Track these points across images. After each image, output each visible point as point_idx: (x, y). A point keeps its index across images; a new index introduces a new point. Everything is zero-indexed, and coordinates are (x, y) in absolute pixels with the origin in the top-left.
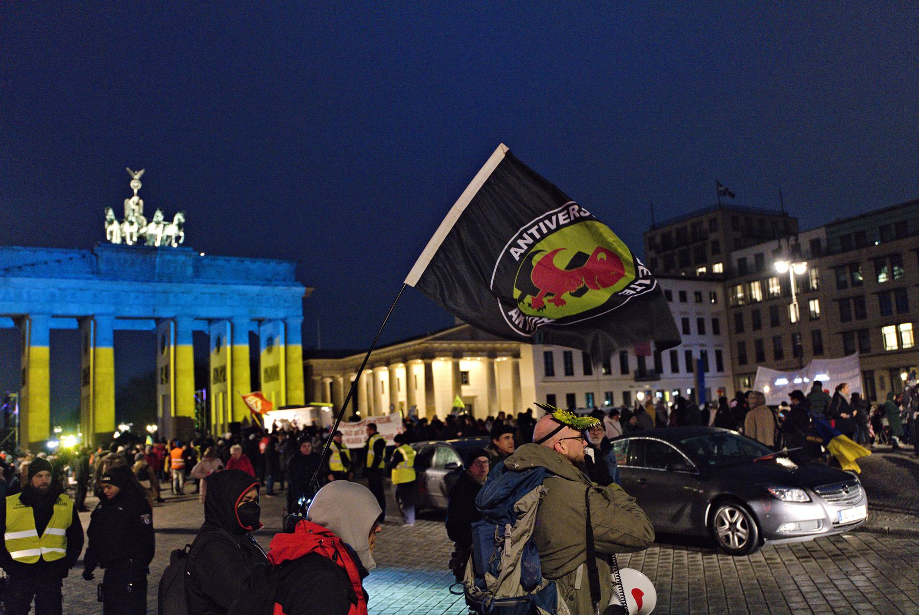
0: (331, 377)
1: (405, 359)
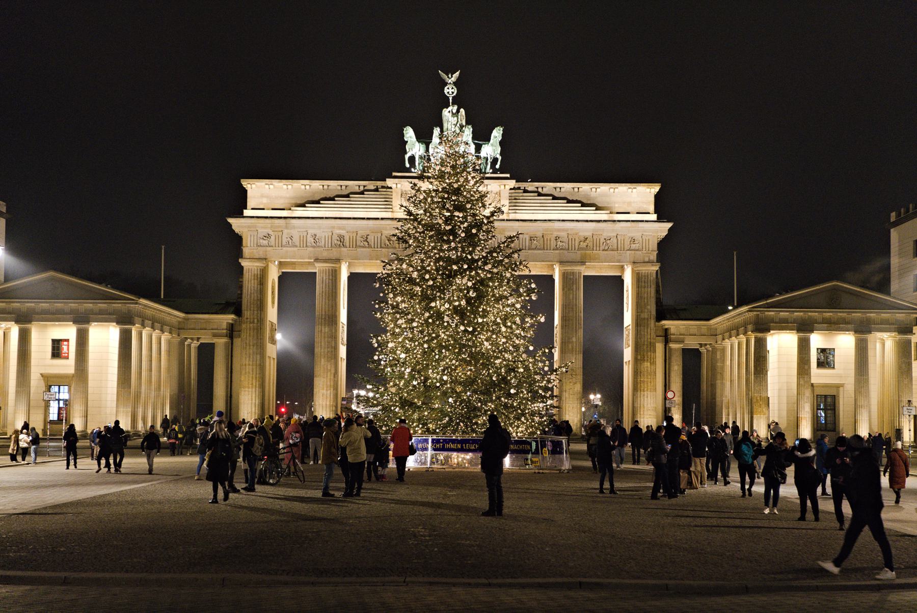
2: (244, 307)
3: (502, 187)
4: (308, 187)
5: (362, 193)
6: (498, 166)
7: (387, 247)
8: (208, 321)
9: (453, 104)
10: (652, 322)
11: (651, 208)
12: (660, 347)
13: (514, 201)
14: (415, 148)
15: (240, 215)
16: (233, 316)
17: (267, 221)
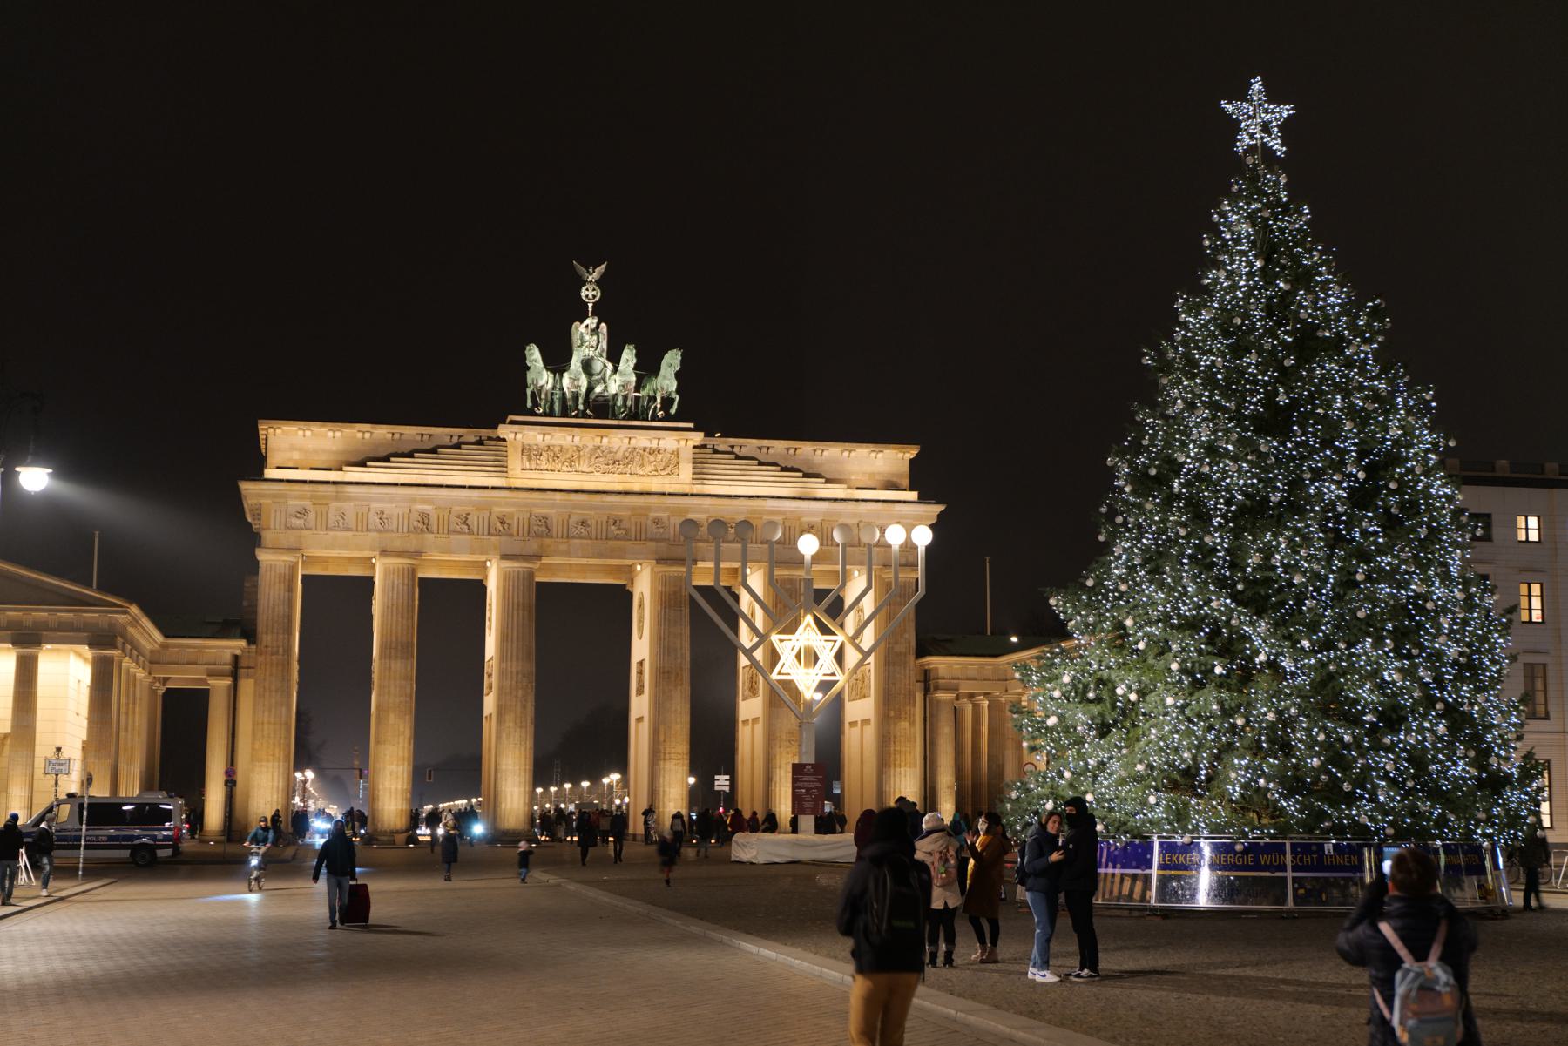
0: (986, 694)
2: (261, 628)
3: (683, 443)
4: (367, 435)
5: (457, 446)
6: (673, 411)
7: (499, 534)
8: (201, 649)
9: (594, 314)
10: (912, 657)
11: (905, 482)
12: (919, 697)
13: (700, 470)
14: (540, 376)
15: (257, 474)
16: (243, 643)
17: (307, 487)
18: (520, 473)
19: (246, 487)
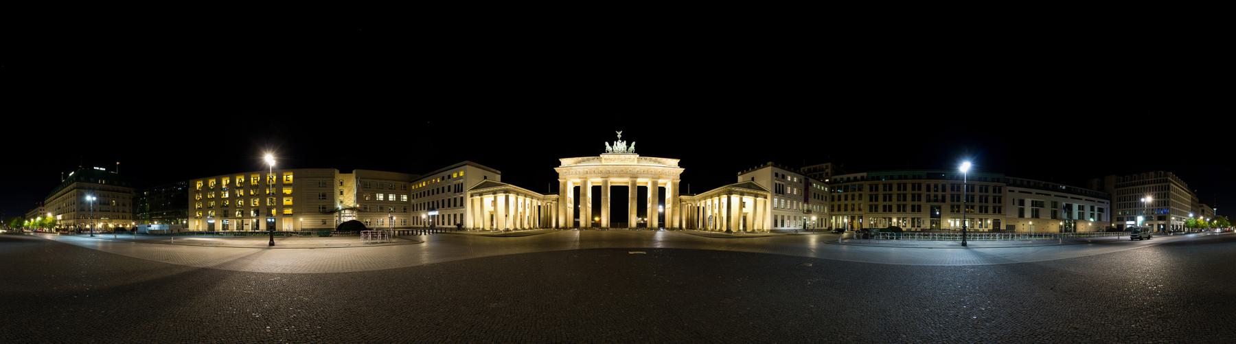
1: (719, 195)
18: (604, 162)
19: (557, 169)
